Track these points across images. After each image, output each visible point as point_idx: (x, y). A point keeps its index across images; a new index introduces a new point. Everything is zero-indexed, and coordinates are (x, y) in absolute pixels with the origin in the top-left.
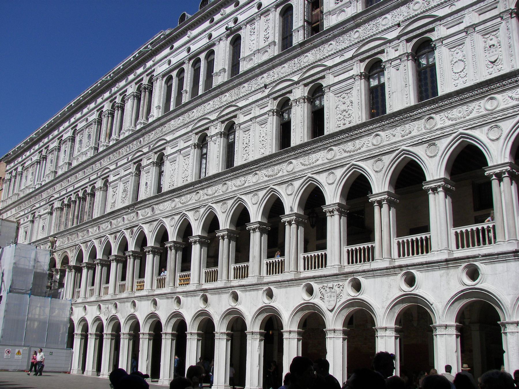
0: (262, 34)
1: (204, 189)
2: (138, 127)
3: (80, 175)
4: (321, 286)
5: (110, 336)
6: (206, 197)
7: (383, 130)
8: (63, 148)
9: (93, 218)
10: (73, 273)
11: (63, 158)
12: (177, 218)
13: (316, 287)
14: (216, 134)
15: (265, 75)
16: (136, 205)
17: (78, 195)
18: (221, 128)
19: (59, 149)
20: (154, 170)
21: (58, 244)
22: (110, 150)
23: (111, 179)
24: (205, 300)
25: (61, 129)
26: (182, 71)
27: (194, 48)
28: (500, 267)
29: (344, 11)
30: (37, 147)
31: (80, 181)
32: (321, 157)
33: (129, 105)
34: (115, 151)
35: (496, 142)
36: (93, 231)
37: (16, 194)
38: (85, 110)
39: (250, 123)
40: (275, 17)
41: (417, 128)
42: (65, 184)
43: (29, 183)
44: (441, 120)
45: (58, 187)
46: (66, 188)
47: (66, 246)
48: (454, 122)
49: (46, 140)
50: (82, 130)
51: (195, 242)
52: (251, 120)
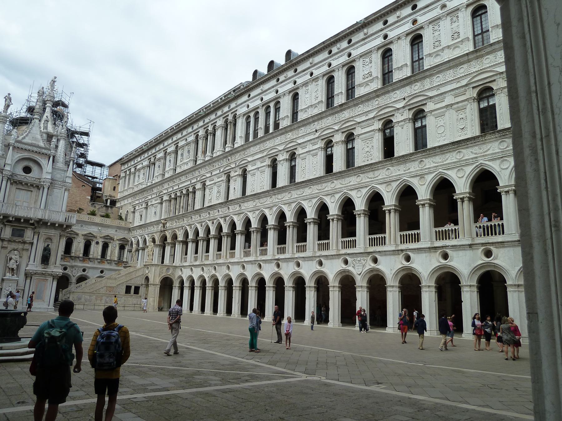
0: (314, 94)
1: (275, 195)
2: (227, 150)
3: (183, 179)
4: (353, 259)
5: (211, 288)
6: (277, 200)
7: (392, 166)
8: (168, 158)
9: (195, 209)
10: (181, 245)
11: (169, 166)
12: (257, 212)
13: (349, 259)
14: (284, 160)
15: (316, 123)
16: (227, 202)
17: (182, 192)
18: (286, 156)
19: (165, 158)
20: (240, 180)
21: (168, 225)
22: (205, 164)
23: (208, 183)
24: (278, 266)
25: (166, 144)
27: (266, 98)
28: (461, 253)
29: (368, 85)
30: (146, 155)
31: (184, 183)
32: (353, 180)
33: (219, 133)
34: (210, 164)
35: (461, 179)
36: (196, 218)
37: (131, 188)
38: (185, 133)
40: (322, 83)
41: (414, 167)
42: (171, 184)
44: (430, 163)
45: (166, 186)
46: (173, 187)
47: (174, 227)
48: (437, 165)
49: (154, 151)
50: (183, 146)
51: (270, 229)
52: (307, 152)
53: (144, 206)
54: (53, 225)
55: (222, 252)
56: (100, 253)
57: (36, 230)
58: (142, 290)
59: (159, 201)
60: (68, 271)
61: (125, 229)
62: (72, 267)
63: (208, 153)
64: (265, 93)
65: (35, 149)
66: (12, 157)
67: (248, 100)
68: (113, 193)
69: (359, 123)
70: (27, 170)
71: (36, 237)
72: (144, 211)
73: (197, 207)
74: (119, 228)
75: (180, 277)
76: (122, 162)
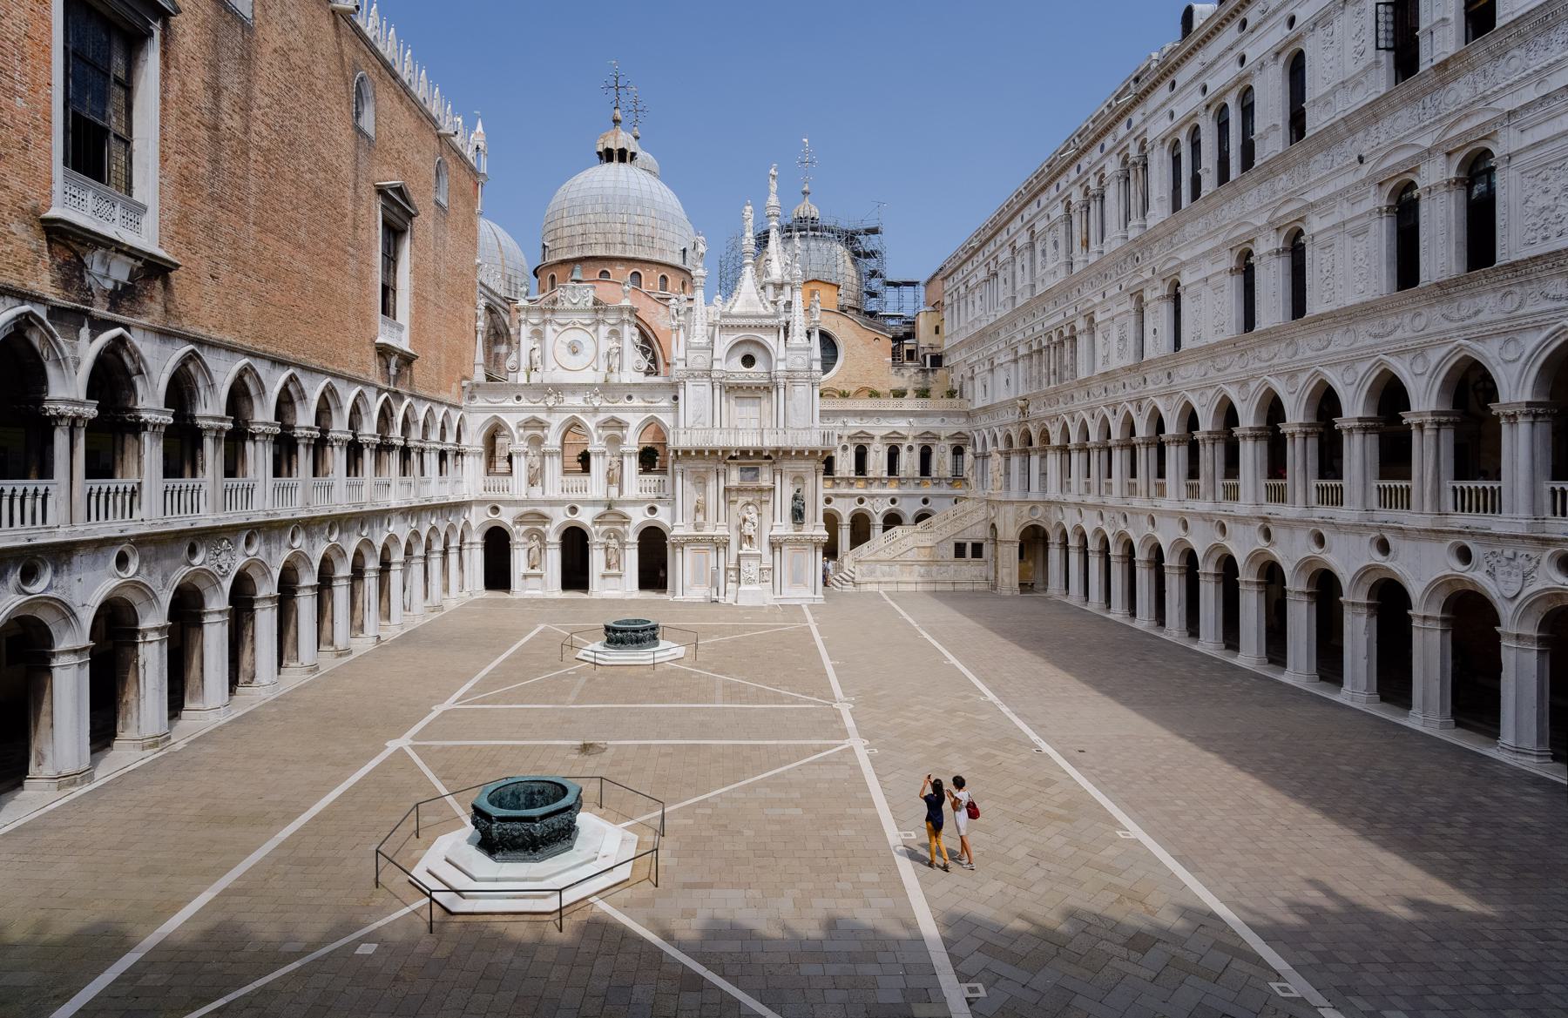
6: (1258, 364)
8: (1018, 259)
16: (1140, 365)
20: (1166, 309)
21: (1031, 409)
23: (1098, 318)
26: (1196, 129)
27: (1215, 83)
33: (1112, 193)
38: (1043, 199)
39: (1334, 232)
43: (978, 313)
49: (991, 247)
51: (1244, 437)
53: (987, 367)
54: (800, 453)
55: (1137, 481)
56: (918, 468)
57: (777, 466)
58: (987, 550)
59: (1012, 357)
60: (866, 506)
61: (958, 414)
62: (872, 496)
63: (1094, 247)
64: (1210, 72)
65: (753, 322)
66: (724, 342)
67: (1170, 100)
68: (935, 340)
69: (1510, 114)
70: (748, 361)
71: (778, 478)
72: (989, 376)
73: (1083, 373)
74: (947, 414)
75: (1060, 524)
76: (943, 274)
